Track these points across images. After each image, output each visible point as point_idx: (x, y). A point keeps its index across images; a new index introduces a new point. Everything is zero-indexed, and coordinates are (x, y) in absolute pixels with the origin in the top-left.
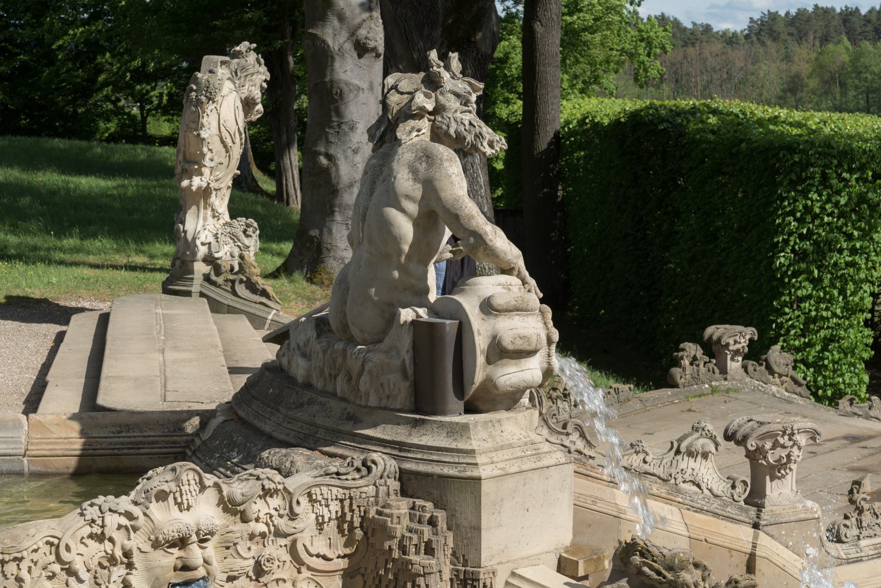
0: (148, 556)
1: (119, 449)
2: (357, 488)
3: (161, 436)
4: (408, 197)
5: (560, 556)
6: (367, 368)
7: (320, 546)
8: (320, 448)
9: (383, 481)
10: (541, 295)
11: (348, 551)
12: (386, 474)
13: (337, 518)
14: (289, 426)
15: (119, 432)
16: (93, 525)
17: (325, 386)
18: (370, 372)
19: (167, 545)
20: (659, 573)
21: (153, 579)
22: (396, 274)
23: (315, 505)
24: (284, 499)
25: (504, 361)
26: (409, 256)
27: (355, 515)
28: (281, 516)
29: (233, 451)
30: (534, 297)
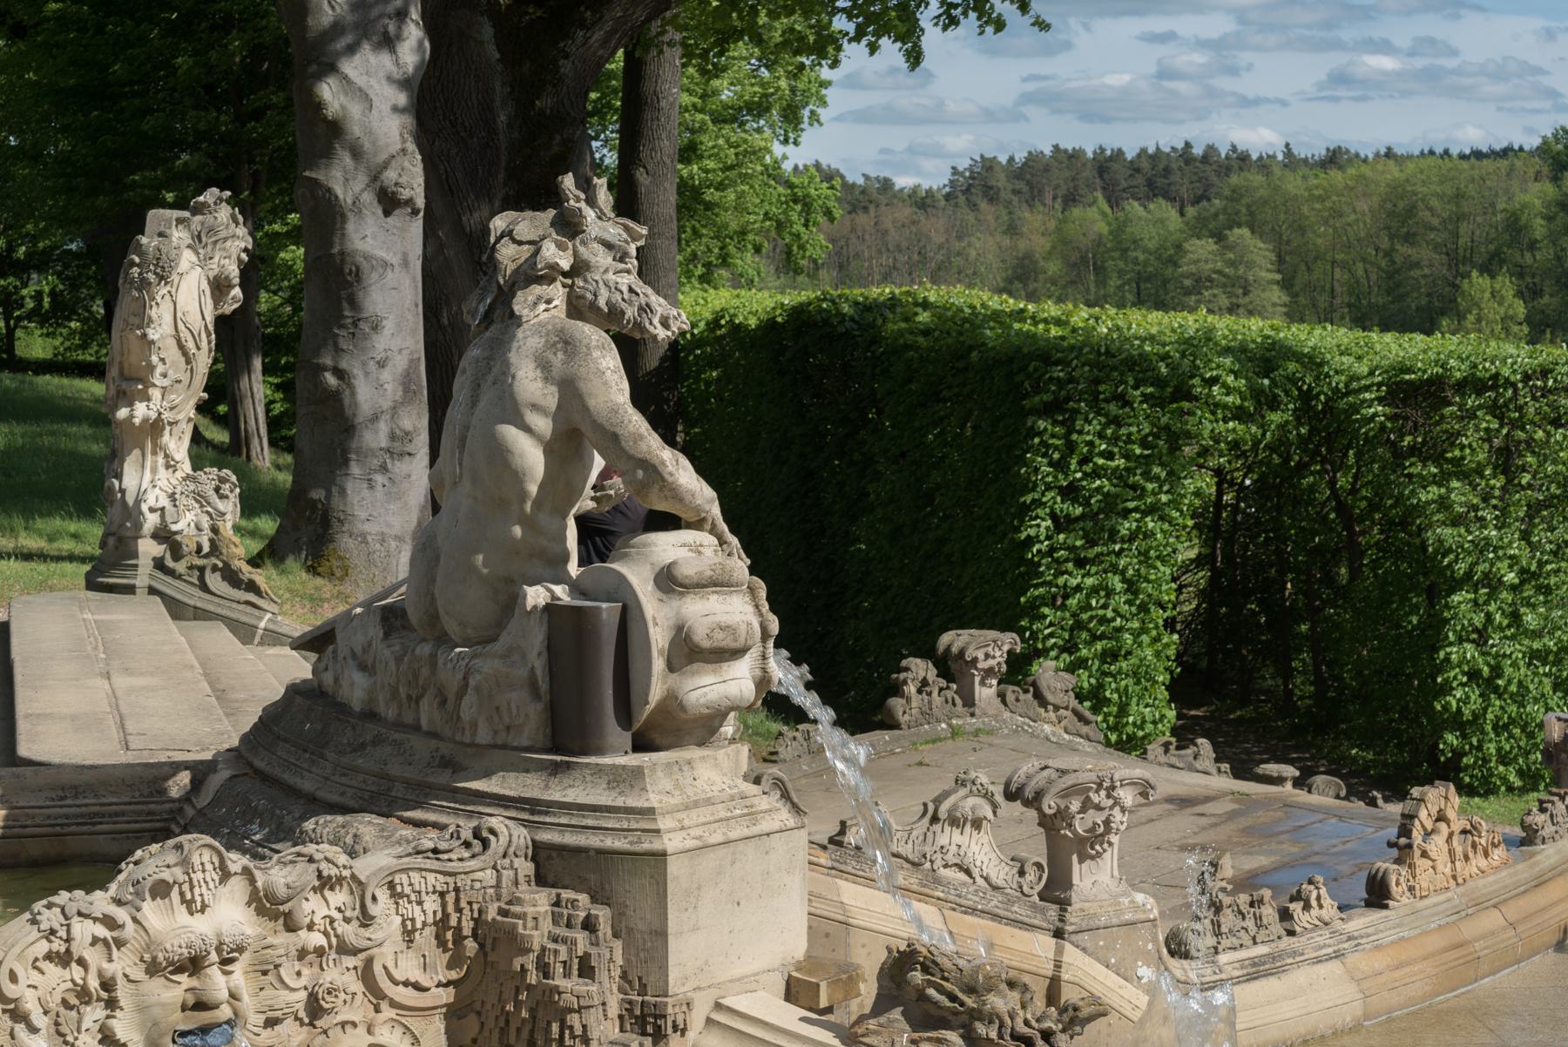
0: (142, 987)
1: (61, 825)
2: (466, 873)
3: (130, 804)
4: (535, 407)
5: (790, 976)
6: (472, 683)
7: (409, 968)
8: (399, 813)
9: (507, 861)
10: (749, 561)
11: (454, 975)
12: (512, 850)
13: (435, 923)
14: (344, 780)
15: (62, 799)
16: (52, 938)
17: (400, 714)
18: (477, 689)
19: (171, 968)
20: (953, 998)
21: (150, 1025)
22: (517, 531)
23: (401, 901)
24: (352, 893)
25: (696, 666)
26: (537, 503)
27: (464, 917)
28: (347, 920)
29: (251, 822)
30: (740, 566)
